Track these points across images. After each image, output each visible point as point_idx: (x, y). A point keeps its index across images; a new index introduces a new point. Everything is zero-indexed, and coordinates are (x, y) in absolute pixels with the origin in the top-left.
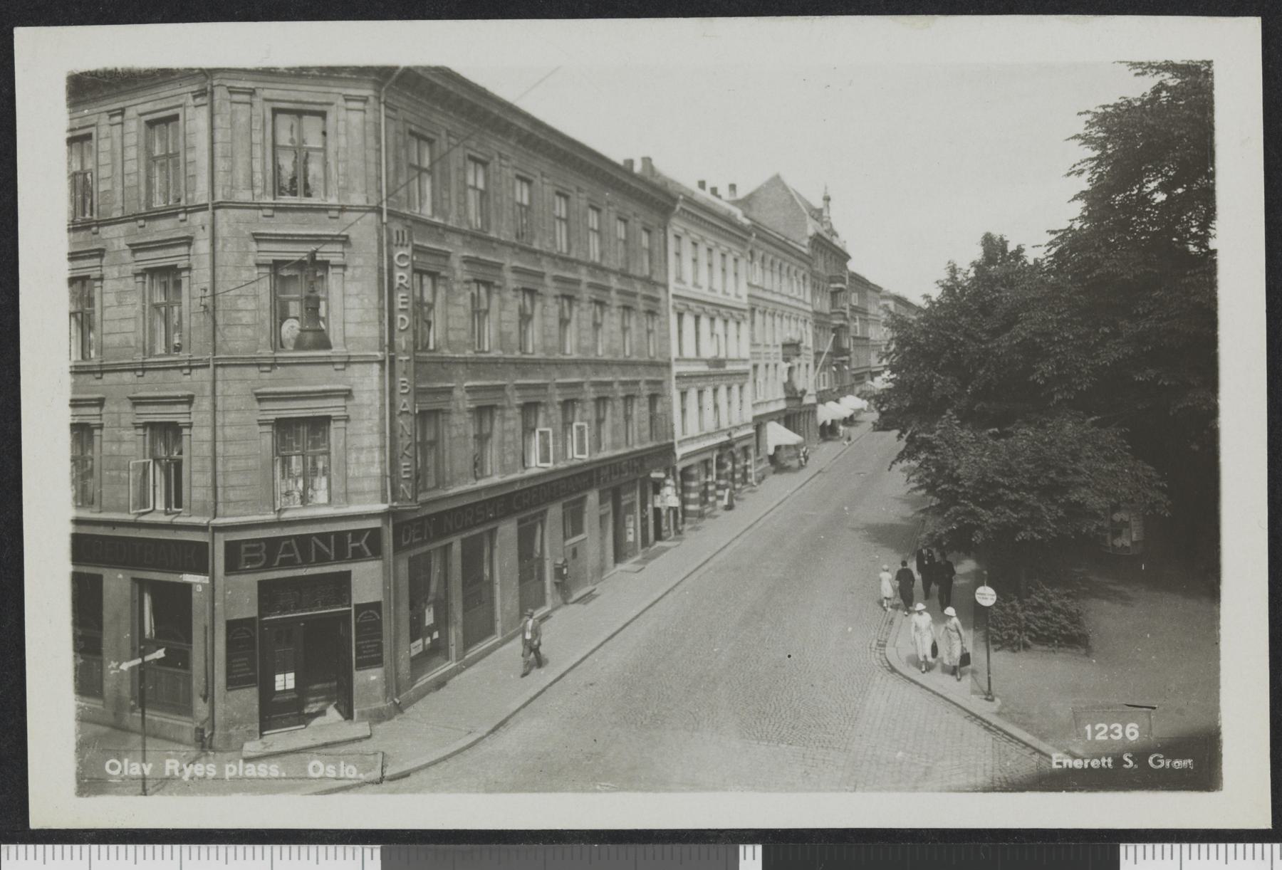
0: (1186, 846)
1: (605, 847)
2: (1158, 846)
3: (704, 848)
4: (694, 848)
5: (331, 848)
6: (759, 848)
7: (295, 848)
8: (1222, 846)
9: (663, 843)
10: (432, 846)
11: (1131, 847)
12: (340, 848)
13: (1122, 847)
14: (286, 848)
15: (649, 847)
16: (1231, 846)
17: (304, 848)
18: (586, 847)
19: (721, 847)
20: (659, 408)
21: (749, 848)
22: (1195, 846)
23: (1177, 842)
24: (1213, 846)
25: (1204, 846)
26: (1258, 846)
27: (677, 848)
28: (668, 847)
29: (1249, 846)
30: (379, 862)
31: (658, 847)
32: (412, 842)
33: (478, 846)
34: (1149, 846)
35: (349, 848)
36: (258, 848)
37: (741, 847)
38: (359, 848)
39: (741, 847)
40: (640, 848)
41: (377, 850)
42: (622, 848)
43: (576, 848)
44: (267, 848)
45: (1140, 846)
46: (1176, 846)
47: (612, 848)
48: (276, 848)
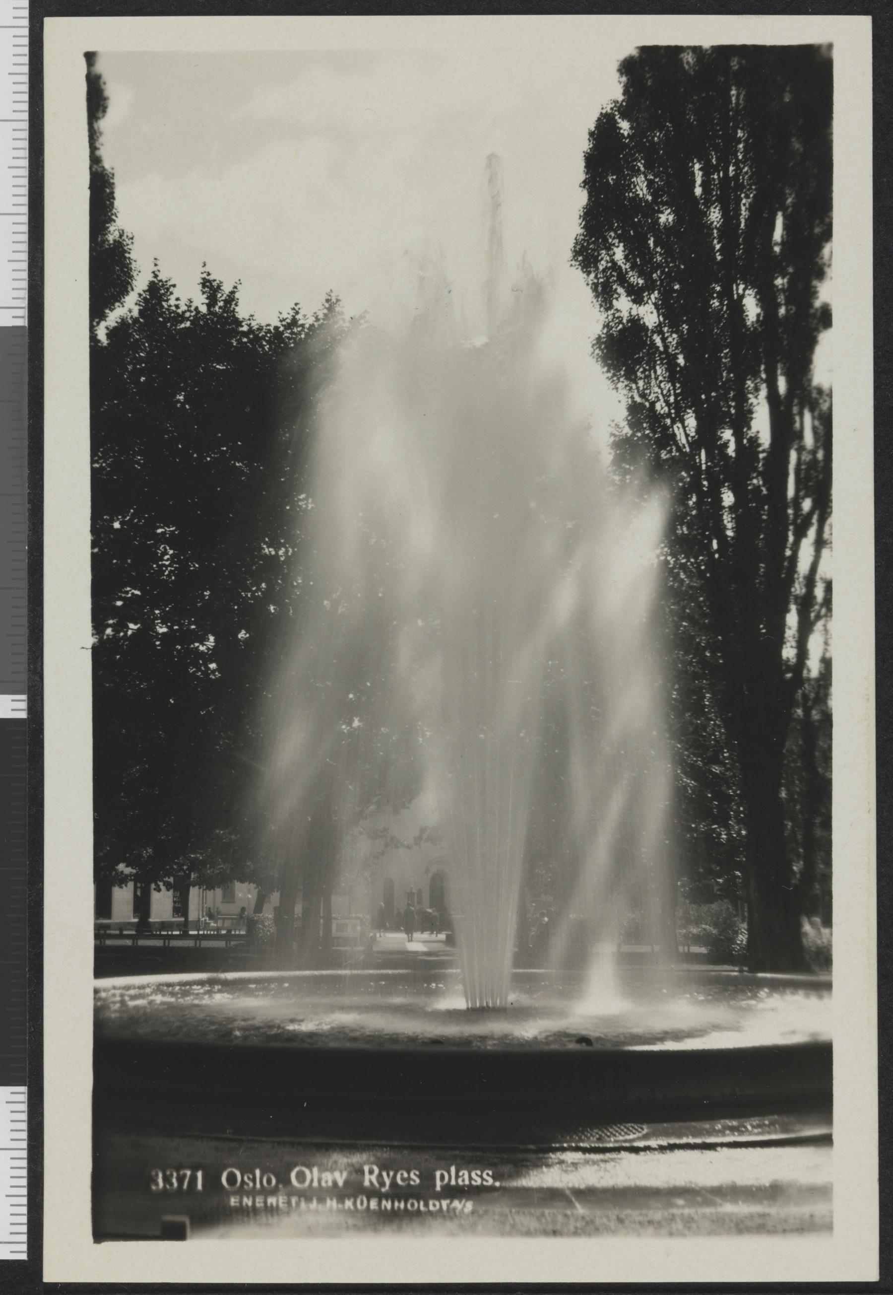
0: (25, 1154)
1: (25, 557)
2: (24, 1126)
3: (24, 658)
4: (24, 649)
5: (25, 275)
6: (23, 715)
7: (25, 238)
8: (25, 1191)
9: (29, 617)
10: (26, 379)
11: (24, 1098)
12: (25, 284)
13: (24, 1089)
14: (25, 228)
15: (24, 602)
16: (25, 1201)
17: (25, 247)
18: (24, 537)
19: (24, 677)
20: (749, 1223)
21: (24, 705)
22: (24, 1163)
23: (29, 1145)
24: (24, 1182)
25: (24, 1173)
26: (24, 1229)
27: (24, 631)
28: (25, 621)
29: (25, 1219)
30: (10, 325)
31: (25, 612)
32: (30, 360)
33: (26, 424)
34: (24, 1116)
35: (25, 294)
36: (25, 200)
37: (24, 697)
38: (25, 303)
39: (24, 697)
40: (24, 593)
41: (23, 322)
42: (24, 574)
43: (24, 528)
44: (25, 209)
45: (24, 1107)
46: (24, 1144)
47: (25, 565)
48: (25, 219)
